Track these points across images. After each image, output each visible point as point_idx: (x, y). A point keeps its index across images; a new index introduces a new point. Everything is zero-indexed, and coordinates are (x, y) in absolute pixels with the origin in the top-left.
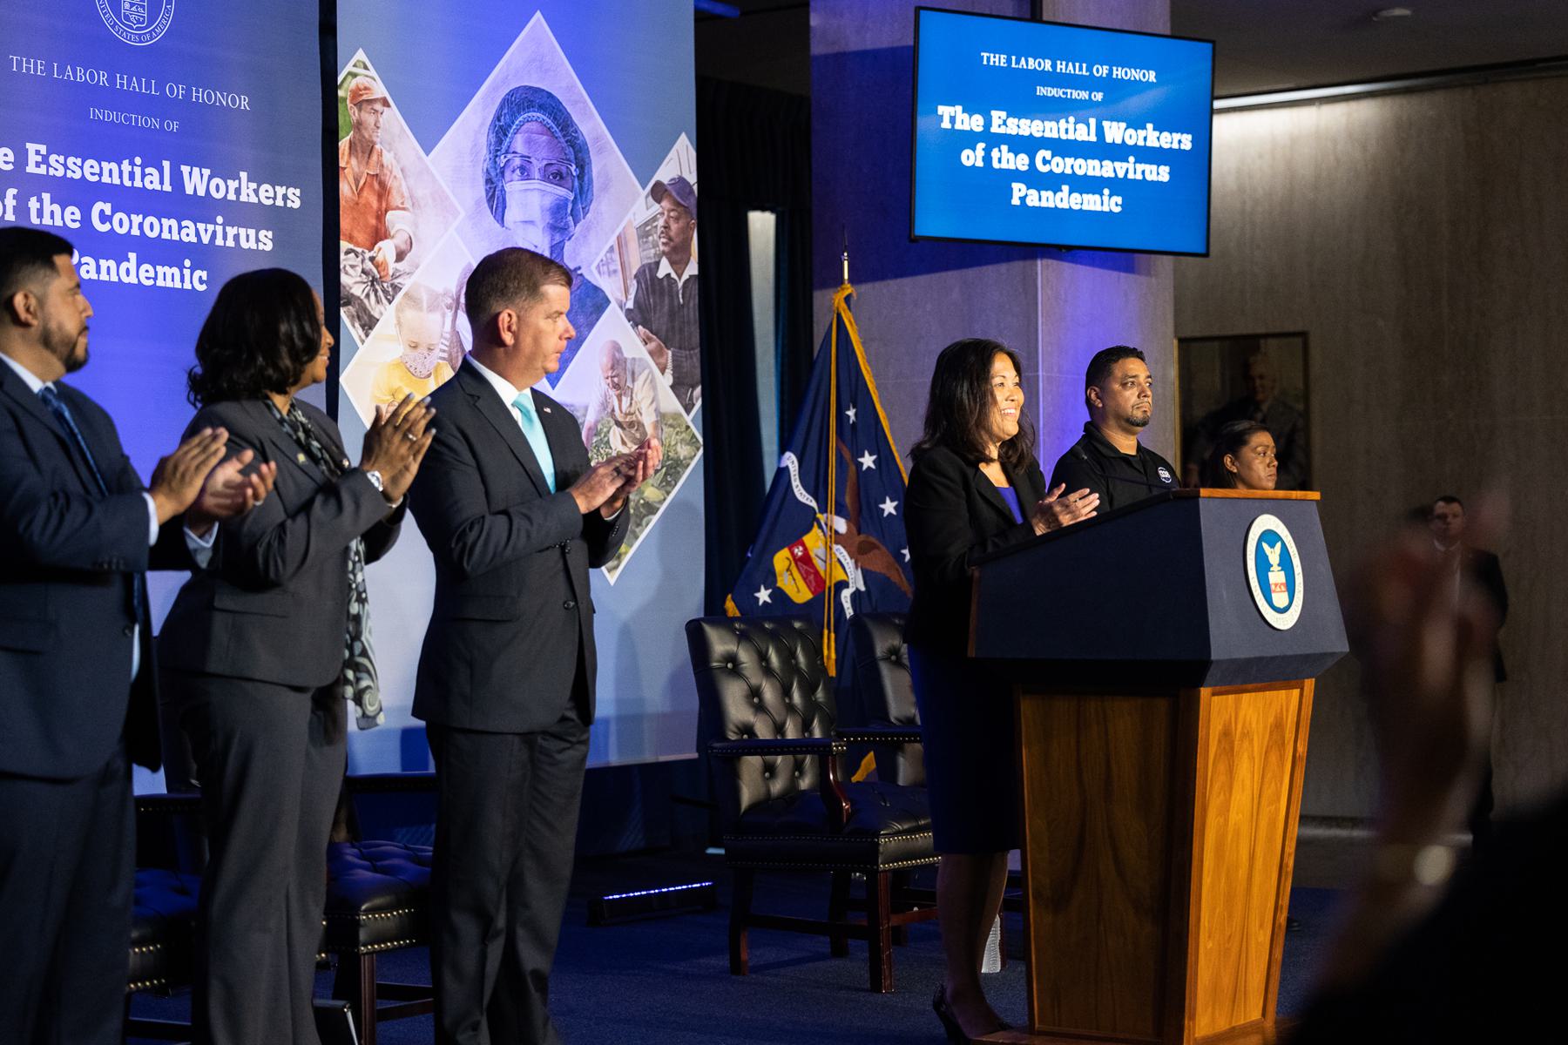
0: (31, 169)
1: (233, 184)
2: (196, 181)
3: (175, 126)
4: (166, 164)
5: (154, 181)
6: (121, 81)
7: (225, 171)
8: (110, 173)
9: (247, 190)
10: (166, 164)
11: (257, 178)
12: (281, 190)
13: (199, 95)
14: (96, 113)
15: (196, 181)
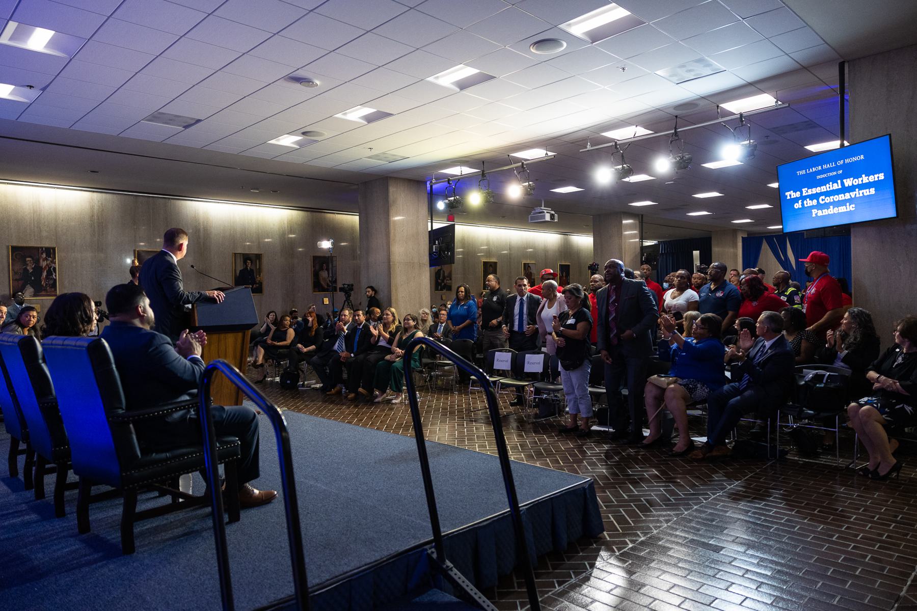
0: (804, 194)
1: (860, 179)
2: (848, 182)
3: (841, 172)
4: (839, 181)
5: (836, 186)
6: (825, 167)
7: (857, 176)
8: (823, 189)
9: (865, 179)
10: (839, 181)
11: (868, 175)
12: (876, 176)
13: (847, 161)
14: (818, 177)
15: (848, 182)
